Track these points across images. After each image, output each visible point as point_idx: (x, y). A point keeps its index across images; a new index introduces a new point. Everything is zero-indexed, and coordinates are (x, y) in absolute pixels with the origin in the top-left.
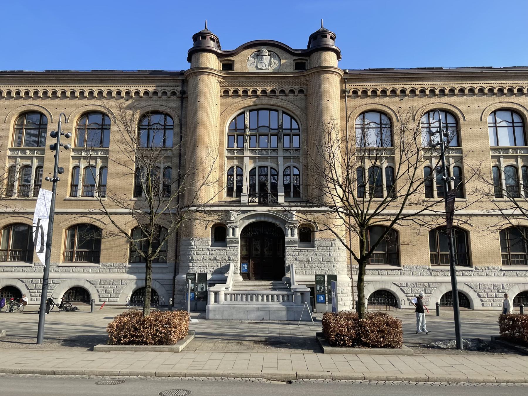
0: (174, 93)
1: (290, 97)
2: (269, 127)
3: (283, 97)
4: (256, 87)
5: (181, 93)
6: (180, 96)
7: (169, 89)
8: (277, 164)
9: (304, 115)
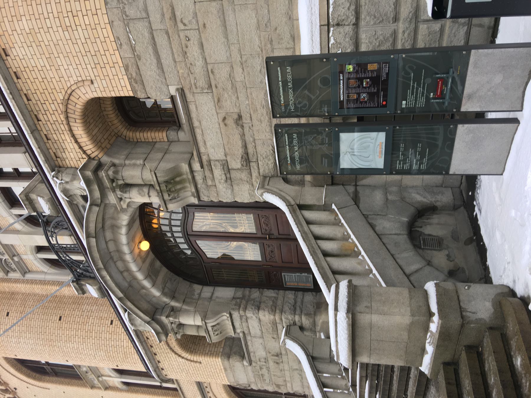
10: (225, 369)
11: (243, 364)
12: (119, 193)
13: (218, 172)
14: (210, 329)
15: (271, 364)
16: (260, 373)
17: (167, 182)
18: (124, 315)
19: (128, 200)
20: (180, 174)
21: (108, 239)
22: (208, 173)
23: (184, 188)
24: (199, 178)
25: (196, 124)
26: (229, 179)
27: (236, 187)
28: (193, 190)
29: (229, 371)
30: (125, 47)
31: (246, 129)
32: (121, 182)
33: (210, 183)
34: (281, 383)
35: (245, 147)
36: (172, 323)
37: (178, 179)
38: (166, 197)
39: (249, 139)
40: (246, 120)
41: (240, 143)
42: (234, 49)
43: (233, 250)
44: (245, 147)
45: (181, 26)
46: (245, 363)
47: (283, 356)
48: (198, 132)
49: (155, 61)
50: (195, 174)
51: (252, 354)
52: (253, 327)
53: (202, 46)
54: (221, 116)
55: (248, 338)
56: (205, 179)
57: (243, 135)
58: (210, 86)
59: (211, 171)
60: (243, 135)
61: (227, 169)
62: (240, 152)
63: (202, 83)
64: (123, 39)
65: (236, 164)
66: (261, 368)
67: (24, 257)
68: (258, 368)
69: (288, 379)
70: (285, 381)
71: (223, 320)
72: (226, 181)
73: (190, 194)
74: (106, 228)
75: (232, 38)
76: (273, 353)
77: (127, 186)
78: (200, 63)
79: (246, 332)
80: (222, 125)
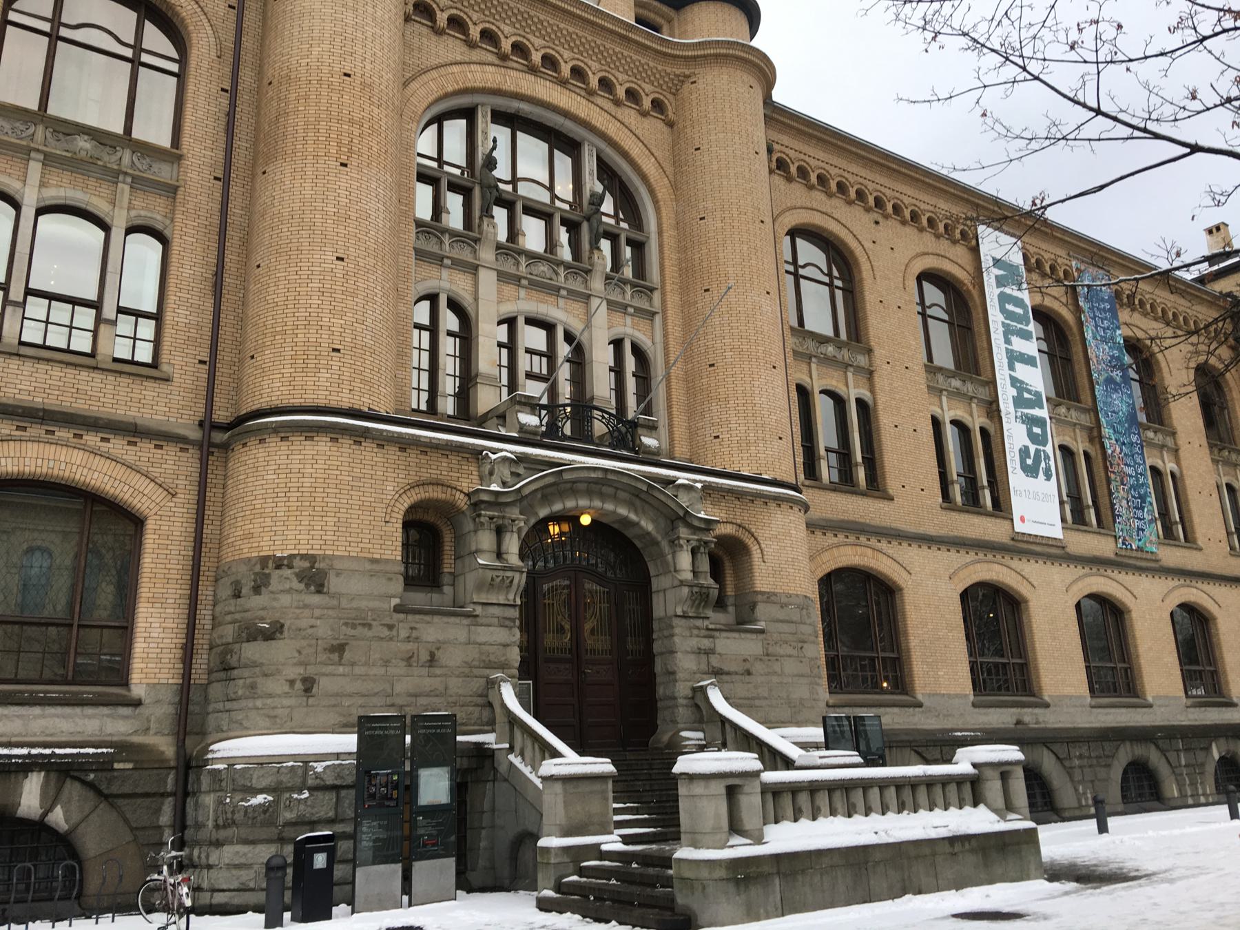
1: (627, 111)
2: (551, 188)
3: (608, 105)
4: (530, 37)
10: (374, 561)
12: (694, 543)
13: (706, 643)
14: (509, 574)
17: (708, 596)
19: (685, 547)
23: (692, 607)
24: (699, 623)
25: (743, 635)
26: (699, 652)
27: (693, 656)
29: (368, 566)
32: (702, 549)
33: (695, 632)
34: (347, 655)
35: (728, 673)
36: (513, 521)
38: (696, 589)
40: (747, 678)
41: (732, 670)
44: (728, 673)
45: (800, 645)
48: (736, 635)
51: (427, 618)
53: (790, 656)
55: (466, 621)
56: (698, 628)
57: (736, 673)
58: (768, 655)
59: (705, 637)
60: (736, 673)
61: (709, 652)
63: (771, 650)
65: (715, 662)
66: (390, 627)
67: (445, 273)
68: (387, 621)
69: (358, 670)
70: (353, 664)
71: (507, 593)
72: (699, 649)
74: (634, 498)
76: (438, 654)
77: (694, 552)
78: (782, 652)
79: (478, 619)
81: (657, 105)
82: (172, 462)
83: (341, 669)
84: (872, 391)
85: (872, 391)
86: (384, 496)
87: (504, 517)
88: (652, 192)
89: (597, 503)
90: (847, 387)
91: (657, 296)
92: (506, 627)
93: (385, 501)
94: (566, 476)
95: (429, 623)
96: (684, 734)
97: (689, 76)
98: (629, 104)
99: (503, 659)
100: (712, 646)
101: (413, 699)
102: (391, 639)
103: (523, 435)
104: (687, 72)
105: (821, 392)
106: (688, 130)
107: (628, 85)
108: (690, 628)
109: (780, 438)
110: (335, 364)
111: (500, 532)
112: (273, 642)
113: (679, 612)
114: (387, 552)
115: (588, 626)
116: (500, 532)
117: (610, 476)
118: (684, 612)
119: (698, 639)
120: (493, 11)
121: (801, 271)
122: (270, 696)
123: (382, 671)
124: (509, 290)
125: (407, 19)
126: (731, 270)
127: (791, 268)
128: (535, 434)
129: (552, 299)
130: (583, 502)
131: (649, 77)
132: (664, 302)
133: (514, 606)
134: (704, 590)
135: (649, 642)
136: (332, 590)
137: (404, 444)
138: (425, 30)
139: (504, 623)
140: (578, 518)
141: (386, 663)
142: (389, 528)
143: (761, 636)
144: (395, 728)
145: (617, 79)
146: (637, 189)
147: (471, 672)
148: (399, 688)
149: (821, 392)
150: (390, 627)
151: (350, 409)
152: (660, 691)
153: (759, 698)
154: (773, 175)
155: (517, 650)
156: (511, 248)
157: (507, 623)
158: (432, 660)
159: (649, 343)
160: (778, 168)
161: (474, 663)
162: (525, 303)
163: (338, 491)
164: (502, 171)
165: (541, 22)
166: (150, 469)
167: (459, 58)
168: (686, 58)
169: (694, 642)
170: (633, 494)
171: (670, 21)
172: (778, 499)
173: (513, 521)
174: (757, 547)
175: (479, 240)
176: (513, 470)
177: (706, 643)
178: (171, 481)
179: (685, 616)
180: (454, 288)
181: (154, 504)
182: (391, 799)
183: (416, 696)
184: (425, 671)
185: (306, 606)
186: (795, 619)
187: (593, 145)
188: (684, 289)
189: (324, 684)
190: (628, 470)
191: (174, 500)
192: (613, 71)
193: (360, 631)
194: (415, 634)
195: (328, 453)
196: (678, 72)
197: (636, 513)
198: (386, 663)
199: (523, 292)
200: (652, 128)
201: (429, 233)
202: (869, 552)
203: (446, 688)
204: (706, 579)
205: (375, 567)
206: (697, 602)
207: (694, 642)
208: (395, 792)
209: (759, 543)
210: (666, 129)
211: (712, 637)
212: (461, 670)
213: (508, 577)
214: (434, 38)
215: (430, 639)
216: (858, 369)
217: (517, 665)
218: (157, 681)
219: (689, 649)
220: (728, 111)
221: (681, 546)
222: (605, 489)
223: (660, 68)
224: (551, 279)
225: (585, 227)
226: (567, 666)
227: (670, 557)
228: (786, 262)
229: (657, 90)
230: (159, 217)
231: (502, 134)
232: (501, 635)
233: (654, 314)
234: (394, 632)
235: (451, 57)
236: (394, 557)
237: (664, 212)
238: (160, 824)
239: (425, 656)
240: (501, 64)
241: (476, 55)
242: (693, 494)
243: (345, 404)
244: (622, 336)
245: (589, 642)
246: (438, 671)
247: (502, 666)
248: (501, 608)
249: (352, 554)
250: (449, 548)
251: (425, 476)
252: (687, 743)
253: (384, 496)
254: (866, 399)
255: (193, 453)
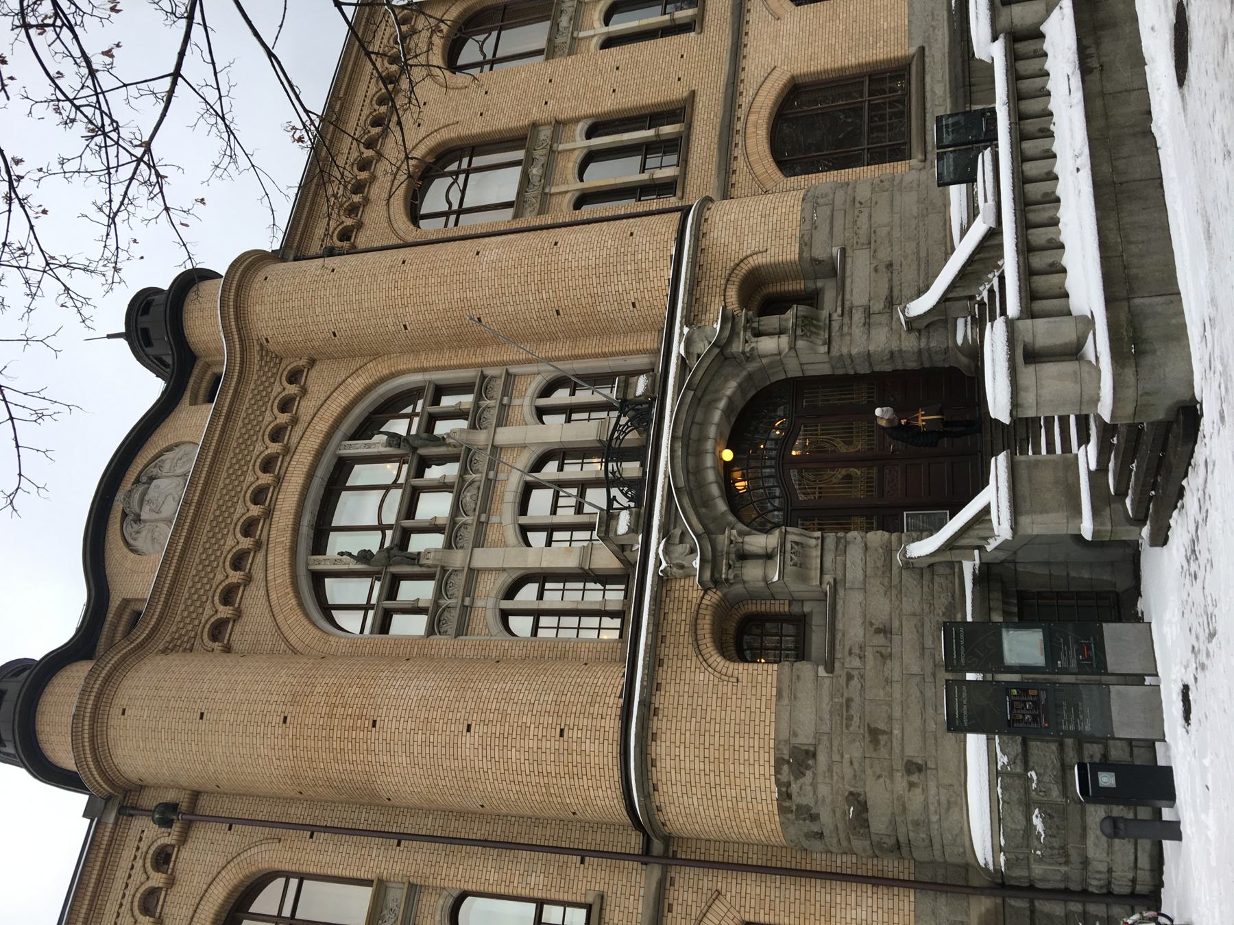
0: (163, 859)
1: (302, 410)
2: (387, 488)
3: (298, 430)
4: (235, 518)
5: (166, 823)
6: (176, 827)
7: (138, 875)
8: (524, 446)
9: (370, 365)
10: (779, 695)
11: (817, 673)
12: (749, 334)
13: (858, 316)
15: (870, 660)
16: (846, 695)
17: (805, 317)
18: (659, 544)
19: (753, 345)
20: (818, 320)
21: (697, 420)
22: (846, 320)
23: (817, 334)
24: (835, 325)
25: (848, 273)
26: (867, 324)
27: (873, 332)
28: (827, 336)
29: (785, 701)
30: (807, 222)
31: (896, 273)
32: (755, 325)
33: (846, 329)
35: (891, 289)
37: (814, 322)
38: (799, 332)
39: (896, 282)
40: (896, 267)
42: (897, 217)
43: (839, 483)
45: (857, 205)
46: (822, 671)
47: (894, 637)
48: (848, 281)
49: (828, 228)
50: (833, 323)
51: (839, 636)
52: (853, 564)
53: (870, 216)
54: (873, 266)
55: (841, 592)
56: (841, 327)
57: (891, 280)
58: (870, 243)
59: (851, 318)
60: (891, 280)
61: (868, 313)
62: (885, 292)
63: (863, 239)
64: (808, 217)
65: (878, 306)
66: (850, 677)
67: (479, 603)
68: (843, 681)
69: (897, 713)
70: (890, 718)
71: (809, 547)
72: (864, 325)
73: (821, 342)
74: (702, 403)
75: (896, 209)
76: (877, 624)
77: (758, 334)
80: (873, 274)
81: (294, 377)
82: (685, 893)
83: (896, 732)
84: (577, 120)
85: (577, 120)
86: (711, 683)
87: (728, 553)
88: (383, 380)
89: (709, 445)
90: (574, 149)
91: (489, 372)
92: (845, 547)
93: (716, 683)
94: (682, 483)
95: (843, 635)
96: (960, 341)
97: (261, 345)
98: (287, 437)
99: (881, 551)
100: (861, 310)
101: (927, 652)
102: (862, 676)
103: (640, 529)
104: (257, 348)
105: (582, 180)
106: (316, 344)
107: (276, 410)
108: (842, 335)
109: (632, 234)
110: (576, 734)
111: (743, 556)
112: (868, 803)
113: (824, 349)
114: (769, 681)
115: (843, 449)
116: (743, 556)
117: (680, 433)
118: (824, 344)
119: (854, 327)
120: (213, 558)
121: (455, 207)
122: (926, 806)
123: (897, 687)
124: (492, 534)
125: (228, 649)
126: (456, 296)
127: (453, 218)
128: (638, 515)
129: (499, 487)
130: (709, 461)
131: (265, 388)
132: (494, 364)
133: (823, 539)
134: (800, 322)
135: (858, 378)
136: (811, 741)
137: (655, 661)
138: (238, 628)
139: (842, 549)
140: (725, 462)
141: (888, 681)
142: (744, 678)
143: (849, 252)
144: (960, 691)
145: (271, 422)
146: (381, 396)
147: (896, 587)
148: (915, 669)
149: (582, 180)
150: (850, 677)
151: (621, 718)
152: (912, 365)
153: (918, 252)
154: (236, 646)
155: (870, 535)
156: (450, 530)
157: (841, 546)
158: (884, 631)
159: (539, 378)
160: (349, 239)
161: (886, 584)
162: (505, 516)
163: (707, 734)
164: (372, 542)
165: (219, 507)
166: (693, 917)
167: (262, 592)
168: (242, 350)
169: (857, 331)
170: (698, 404)
171: (208, 366)
172: (698, 236)
173: (731, 542)
174: (750, 259)
175: (443, 567)
176: (677, 540)
177: (858, 316)
178: (704, 896)
179: (829, 343)
180: (493, 594)
181: (729, 914)
182: (1038, 696)
183: (923, 648)
184: (896, 639)
185: (830, 770)
186: (829, 213)
187: (339, 445)
188: (481, 343)
189: (912, 750)
190: (671, 416)
191: (723, 892)
192: (263, 427)
193: (855, 710)
194: (856, 650)
195: (668, 744)
196: (258, 357)
197: (717, 400)
198: (888, 681)
199: (494, 519)
200: (318, 382)
201: (439, 621)
202: (752, 118)
203: (914, 615)
204: (787, 320)
205: (785, 694)
206: (814, 330)
207: (857, 331)
208: (1031, 692)
209: (746, 257)
210: (317, 367)
211: (851, 309)
212: (894, 598)
213: (792, 548)
214: (244, 619)
215: (860, 632)
216: (555, 138)
217: (887, 534)
218: (912, 914)
219: (865, 337)
220: (292, 304)
221: (752, 349)
222: (694, 434)
223: (255, 377)
224: (479, 488)
225: (422, 451)
226: (887, 471)
227: (764, 361)
228: (446, 226)
229: (278, 379)
230: (441, 902)
231: (338, 543)
232: (855, 554)
233: (508, 373)
234: (855, 673)
235: (262, 601)
236: (775, 673)
237: (403, 367)
238: (1063, 914)
239: (880, 640)
240: (265, 547)
241: (258, 574)
242: (695, 336)
243: (617, 724)
244: (533, 408)
245: (859, 447)
246: (896, 624)
247: (889, 551)
248: (826, 553)
249: (773, 719)
250: (763, 606)
251: (687, 638)
252: (970, 338)
253: (711, 683)
254: (586, 127)
255: (674, 872)
